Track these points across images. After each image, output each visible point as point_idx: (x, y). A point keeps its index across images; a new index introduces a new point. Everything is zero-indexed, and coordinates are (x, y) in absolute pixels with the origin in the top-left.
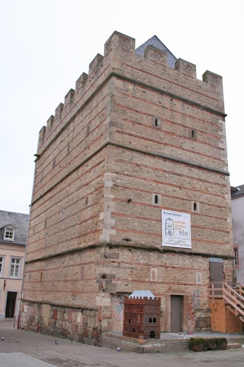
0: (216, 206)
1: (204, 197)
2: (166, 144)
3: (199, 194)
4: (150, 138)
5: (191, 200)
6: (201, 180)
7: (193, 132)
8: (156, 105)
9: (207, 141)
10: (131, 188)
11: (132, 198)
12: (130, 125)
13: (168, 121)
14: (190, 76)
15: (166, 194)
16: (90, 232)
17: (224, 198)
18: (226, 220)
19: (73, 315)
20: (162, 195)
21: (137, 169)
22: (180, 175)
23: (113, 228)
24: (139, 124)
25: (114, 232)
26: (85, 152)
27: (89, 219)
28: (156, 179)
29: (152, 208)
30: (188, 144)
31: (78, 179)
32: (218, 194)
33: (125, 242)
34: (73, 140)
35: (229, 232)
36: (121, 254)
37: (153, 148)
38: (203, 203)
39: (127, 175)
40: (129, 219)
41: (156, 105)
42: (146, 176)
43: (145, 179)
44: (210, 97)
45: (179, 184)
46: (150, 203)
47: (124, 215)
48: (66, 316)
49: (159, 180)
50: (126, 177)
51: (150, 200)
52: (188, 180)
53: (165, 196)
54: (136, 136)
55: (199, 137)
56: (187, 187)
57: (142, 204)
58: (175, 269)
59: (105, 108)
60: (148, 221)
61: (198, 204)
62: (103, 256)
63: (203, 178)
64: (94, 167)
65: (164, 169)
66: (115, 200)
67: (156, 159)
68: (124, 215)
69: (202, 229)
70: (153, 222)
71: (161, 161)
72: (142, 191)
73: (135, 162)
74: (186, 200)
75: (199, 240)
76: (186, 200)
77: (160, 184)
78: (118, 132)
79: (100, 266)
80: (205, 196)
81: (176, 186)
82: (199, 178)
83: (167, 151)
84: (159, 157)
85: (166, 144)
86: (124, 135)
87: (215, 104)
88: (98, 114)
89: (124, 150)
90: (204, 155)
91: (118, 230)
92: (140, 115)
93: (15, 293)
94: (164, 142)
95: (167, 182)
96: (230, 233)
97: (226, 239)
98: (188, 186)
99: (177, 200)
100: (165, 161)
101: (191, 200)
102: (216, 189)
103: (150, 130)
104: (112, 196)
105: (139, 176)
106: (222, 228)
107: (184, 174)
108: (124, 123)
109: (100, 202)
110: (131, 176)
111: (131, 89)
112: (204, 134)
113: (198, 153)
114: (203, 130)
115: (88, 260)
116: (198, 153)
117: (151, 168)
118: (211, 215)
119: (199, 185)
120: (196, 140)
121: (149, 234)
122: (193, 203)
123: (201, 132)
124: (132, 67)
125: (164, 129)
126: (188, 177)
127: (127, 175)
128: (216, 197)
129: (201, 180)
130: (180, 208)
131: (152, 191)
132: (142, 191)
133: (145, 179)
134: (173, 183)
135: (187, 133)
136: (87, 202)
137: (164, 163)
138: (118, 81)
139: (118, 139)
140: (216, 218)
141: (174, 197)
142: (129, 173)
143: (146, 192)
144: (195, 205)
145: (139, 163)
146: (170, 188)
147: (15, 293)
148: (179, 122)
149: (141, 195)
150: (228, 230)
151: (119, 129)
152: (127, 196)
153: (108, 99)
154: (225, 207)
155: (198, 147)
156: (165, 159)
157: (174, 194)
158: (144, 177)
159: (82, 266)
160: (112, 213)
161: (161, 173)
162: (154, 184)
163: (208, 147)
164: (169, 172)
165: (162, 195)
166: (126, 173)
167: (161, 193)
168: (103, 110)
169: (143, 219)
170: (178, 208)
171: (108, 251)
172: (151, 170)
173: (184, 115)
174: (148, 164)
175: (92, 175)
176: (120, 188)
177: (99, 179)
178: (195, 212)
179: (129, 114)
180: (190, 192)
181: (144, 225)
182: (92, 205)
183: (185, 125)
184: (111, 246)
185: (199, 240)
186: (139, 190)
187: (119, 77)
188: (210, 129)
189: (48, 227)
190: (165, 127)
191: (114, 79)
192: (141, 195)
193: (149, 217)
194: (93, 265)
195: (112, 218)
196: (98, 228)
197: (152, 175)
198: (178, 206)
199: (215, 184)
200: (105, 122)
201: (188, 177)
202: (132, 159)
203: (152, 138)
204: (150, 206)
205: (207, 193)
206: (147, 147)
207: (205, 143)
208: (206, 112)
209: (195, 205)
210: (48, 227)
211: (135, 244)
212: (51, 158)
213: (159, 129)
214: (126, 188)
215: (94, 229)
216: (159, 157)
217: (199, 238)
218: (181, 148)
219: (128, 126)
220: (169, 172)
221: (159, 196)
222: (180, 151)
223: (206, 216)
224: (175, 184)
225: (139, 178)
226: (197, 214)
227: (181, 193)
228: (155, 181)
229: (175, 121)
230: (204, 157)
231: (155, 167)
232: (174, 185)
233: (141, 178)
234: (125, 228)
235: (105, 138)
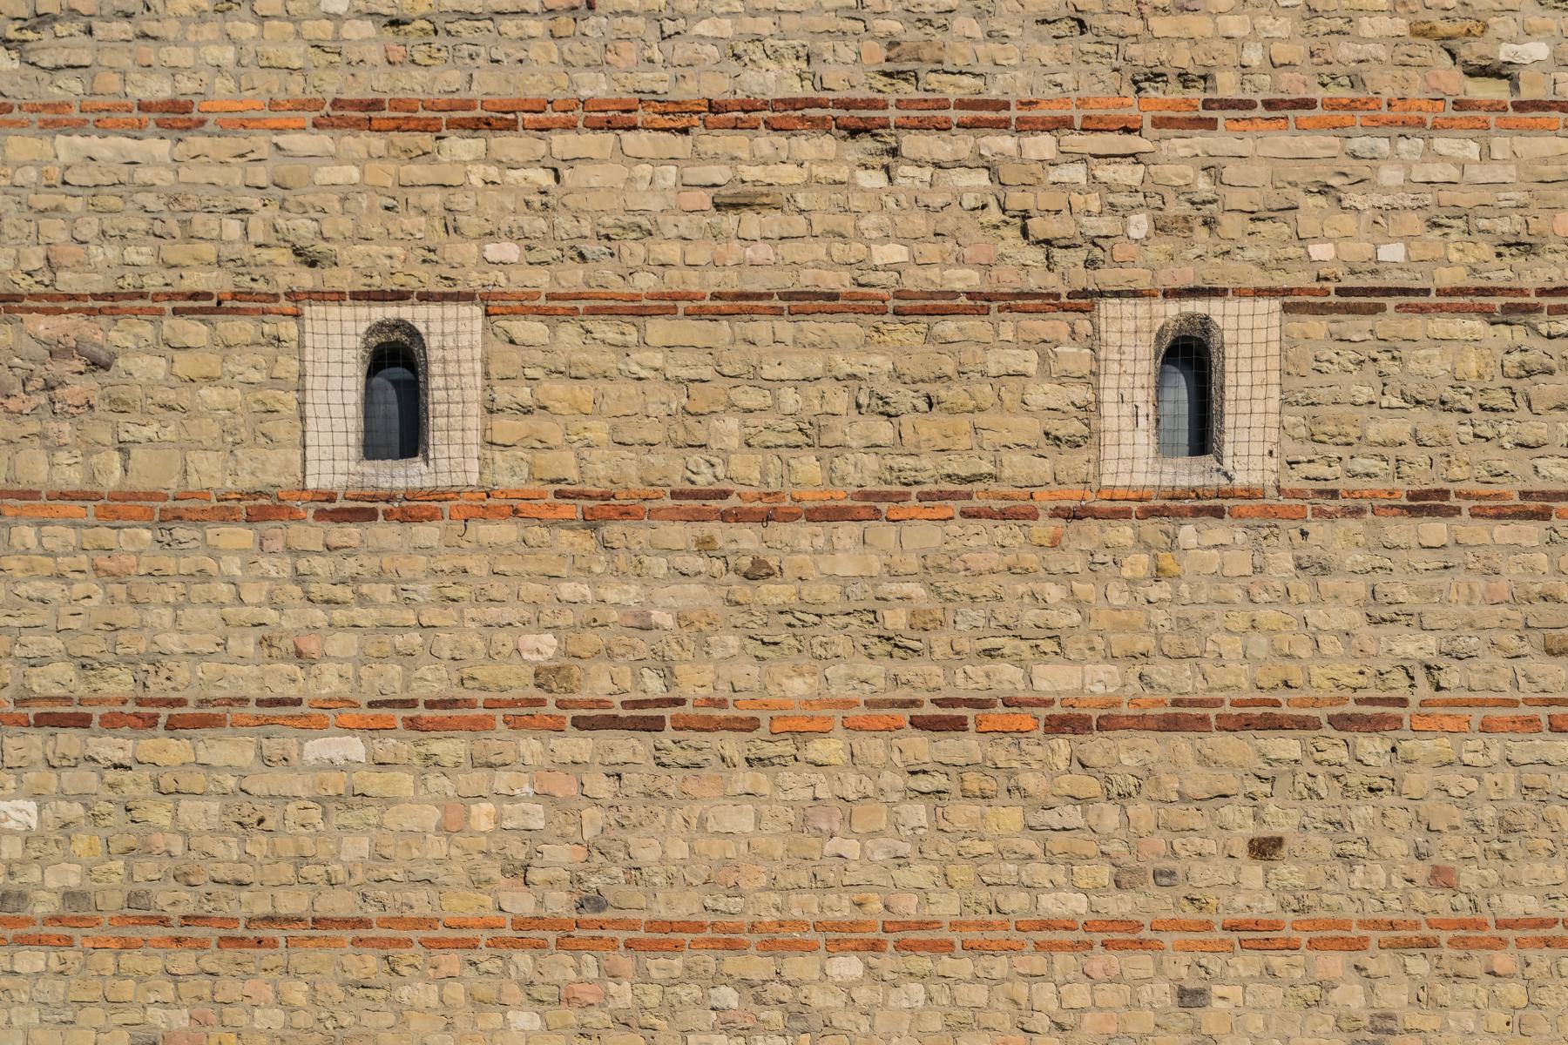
3: (1257, 156)
5: (1084, 300)
15: (574, 277)
20: (494, 304)
28: (376, 83)
29: (310, 534)
43: (176, 116)
46: (269, 469)
51: (279, 409)
53: (555, 308)
60: (229, 750)
74: (980, 303)
75: (1255, 934)
76: (980, 303)
77: (461, 147)
81: (787, 116)
95: (594, 86)
101: (1084, 300)
105: (70, 87)
130: (862, 470)
132: (111, 303)
133: (176, 116)
141: (740, 304)
143: (200, 304)
149: (98, 365)
157: (756, 253)
158: (159, 88)
162: (342, 163)
167: (474, 280)
169: (143, 716)
170: (808, 467)
181: (159, 815)
185: (1255, 934)
186: (55, 302)
192: (98, 365)
193: (250, 677)
198: (811, 434)
221: (453, 339)
225: (56, 119)
228: (362, 114)
233: (100, 118)
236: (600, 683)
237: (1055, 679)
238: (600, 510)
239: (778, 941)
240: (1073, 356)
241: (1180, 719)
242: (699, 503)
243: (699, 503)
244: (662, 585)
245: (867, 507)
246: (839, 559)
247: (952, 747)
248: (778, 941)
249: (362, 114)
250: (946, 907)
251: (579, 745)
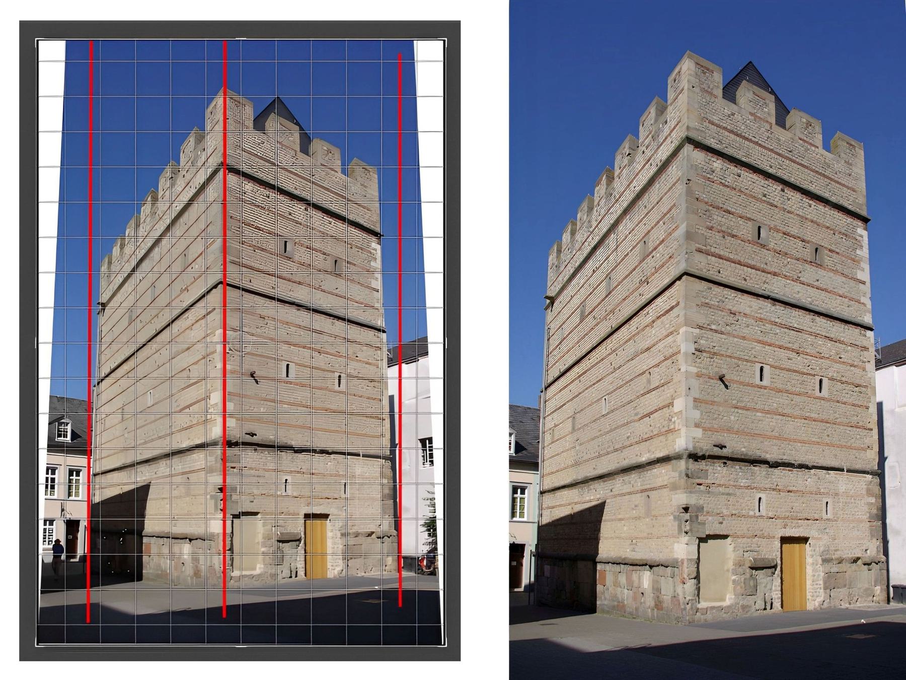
1: (835, 370)
2: (775, 274)
4: (750, 262)
5: (814, 375)
6: (831, 339)
7: (816, 250)
8: (757, 199)
9: (839, 267)
10: (722, 355)
11: (724, 372)
12: (718, 236)
13: (778, 231)
14: (811, 144)
16: (658, 435)
17: (864, 369)
18: (867, 408)
19: (635, 576)
21: (731, 319)
22: (799, 331)
23: (697, 425)
24: (733, 236)
25: (698, 433)
26: (641, 290)
27: (656, 411)
28: (761, 338)
30: (810, 273)
31: (630, 339)
32: (856, 363)
33: (716, 449)
34: (616, 267)
36: (710, 471)
37: (755, 282)
39: (716, 331)
40: (721, 409)
41: (757, 199)
42: (746, 332)
43: (744, 338)
44: (844, 185)
45: (796, 346)
47: (713, 403)
48: (623, 579)
49: (765, 339)
50: (715, 334)
52: (810, 339)
55: (827, 260)
56: (808, 351)
57: (741, 383)
59: (674, 205)
61: (825, 381)
62: (683, 475)
63: (832, 336)
64: (658, 318)
65: (773, 319)
66: (699, 375)
67: (761, 302)
68: (713, 403)
69: (832, 425)
70: (759, 414)
71: (767, 304)
72: (739, 359)
73: (727, 307)
74: (807, 374)
76: (807, 374)
78: (700, 251)
79: (678, 491)
80: (837, 366)
81: (793, 350)
82: (827, 335)
83: (777, 287)
84: (767, 297)
85: (775, 274)
86: (709, 257)
87: (851, 199)
88: (664, 216)
89: (711, 285)
90: (835, 293)
91: (705, 430)
93: (522, 547)
94: (772, 270)
95: (777, 343)
99: (795, 376)
100: (774, 305)
101: (814, 375)
102: (850, 355)
103: (749, 248)
104: (694, 370)
105: (734, 332)
106: (861, 424)
107: (805, 328)
108: (709, 233)
109: (674, 381)
110: (722, 333)
111: (718, 170)
112: (834, 255)
113: (826, 290)
114: (833, 248)
115: (659, 482)
116: (826, 290)
117: (754, 318)
118: (845, 400)
119: (828, 348)
120: (820, 266)
121: (754, 435)
122: (818, 378)
123: (830, 251)
124: (718, 126)
125: (772, 245)
126: (811, 334)
127: (716, 331)
128: (852, 368)
129: (831, 339)
131: (754, 359)
132: (739, 359)
133: (744, 338)
135: (808, 253)
136: (649, 381)
138: (696, 151)
139: (701, 264)
140: (853, 405)
141: (789, 370)
142: (719, 328)
143: (747, 361)
144: (821, 381)
145: (734, 309)
146: (783, 354)
147: (522, 547)
148: (794, 231)
150: (869, 426)
151: (700, 246)
152: (717, 369)
153: (681, 188)
154: (866, 387)
155: (826, 278)
159: (647, 493)
160: (695, 400)
161: (768, 326)
162: (759, 347)
163: (840, 279)
164: (781, 326)
165: (772, 366)
166: (713, 327)
168: (670, 210)
171: (693, 466)
173: (803, 218)
174: (748, 311)
175: (656, 332)
176: (704, 354)
177: (670, 339)
178: (821, 395)
182: (657, 388)
183: (805, 238)
184: (695, 457)
186: (735, 358)
187: (699, 145)
188: (843, 245)
189: (579, 429)
190: (774, 240)
191: (688, 148)
194: (665, 492)
195: (696, 407)
196: (672, 427)
197: (755, 330)
199: (852, 345)
200: (676, 234)
201: (811, 334)
203: (753, 263)
204: (752, 385)
205: (840, 363)
206: (745, 280)
207: (836, 272)
208: (836, 213)
209: (821, 381)
210: (579, 429)
211: (733, 452)
212: (576, 301)
213: (763, 246)
214: (715, 354)
215: (667, 429)
216: (767, 297)
217: (827, 440)
218: (797, 280)
219: (716, 242)
220: (781, 326)
222: (798, 287)
223: (838, 402)
224: (790, 345)
225: (734, 336)
226: (823, 399)
227: (799, 362)
228: (759, 342)
229: (789, 230)
230: (835, 296)
231: (759, 316)
232: (788, 349)
233: (737, 337)
234: (716, 426)
235: (678, 263)
236: (780, 410)
237: (813, 415)
238: (780, 391)
239: (795, 441)
241: (822, 421)
242: (787, 391)
244: (783, 399)
245: (799, 395)
246: (797, 399)
247: (806, 421)
248: (795, 441)
250: (806, 439)
251: (778, 417)
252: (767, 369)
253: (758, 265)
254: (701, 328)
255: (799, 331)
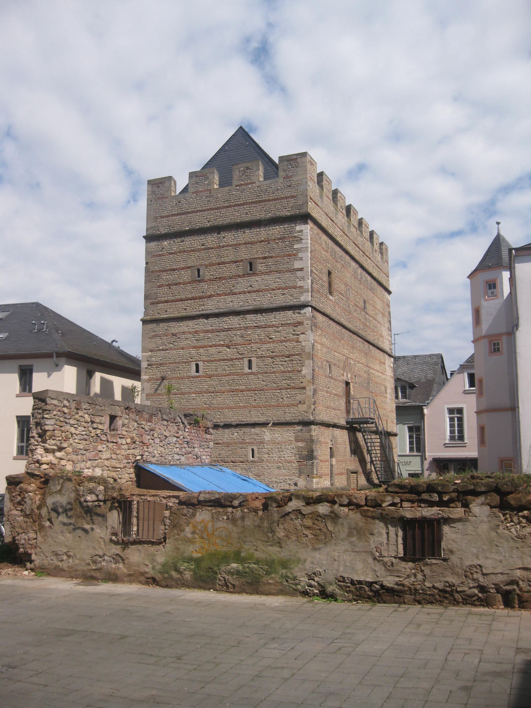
0: (283, 356)
20: (203, 361)
35: (304, 388)
38: (261, 357)
39: (163, 350)
45: (227, 342)
54: (172, 301)
58: (219, 445)
73: (171, 332)
76: (236, 359)
81: (223, 346)
83: (211, 306)
92: (178, 273)
96: (307, 388)
97: (299, 397)
98: (239, 340)
110: (167, 350)
119: (253, 334)
127: (163, 350)
132: (178, 363)
133: (183, 348)
134: (218, 343)
137: (206, 321)
142: (165, 347)
146: (213, 350)
156: (207, 316)
165: (203, 361)
172: (190, 336)
174: (186, 329)
179: (164, 277)
180: (241, 349)
202: (168, 330)
205: (269, 342)
206: (185, 309)
224: (222, 343)
228: (195, 347)
240: (242, 362)
242: (217, 375)
243: (217, 375)
249: (195, 347)
252: (201, 364)
253: (197, 295)
254: (151, 351)
255: (229, 330)
